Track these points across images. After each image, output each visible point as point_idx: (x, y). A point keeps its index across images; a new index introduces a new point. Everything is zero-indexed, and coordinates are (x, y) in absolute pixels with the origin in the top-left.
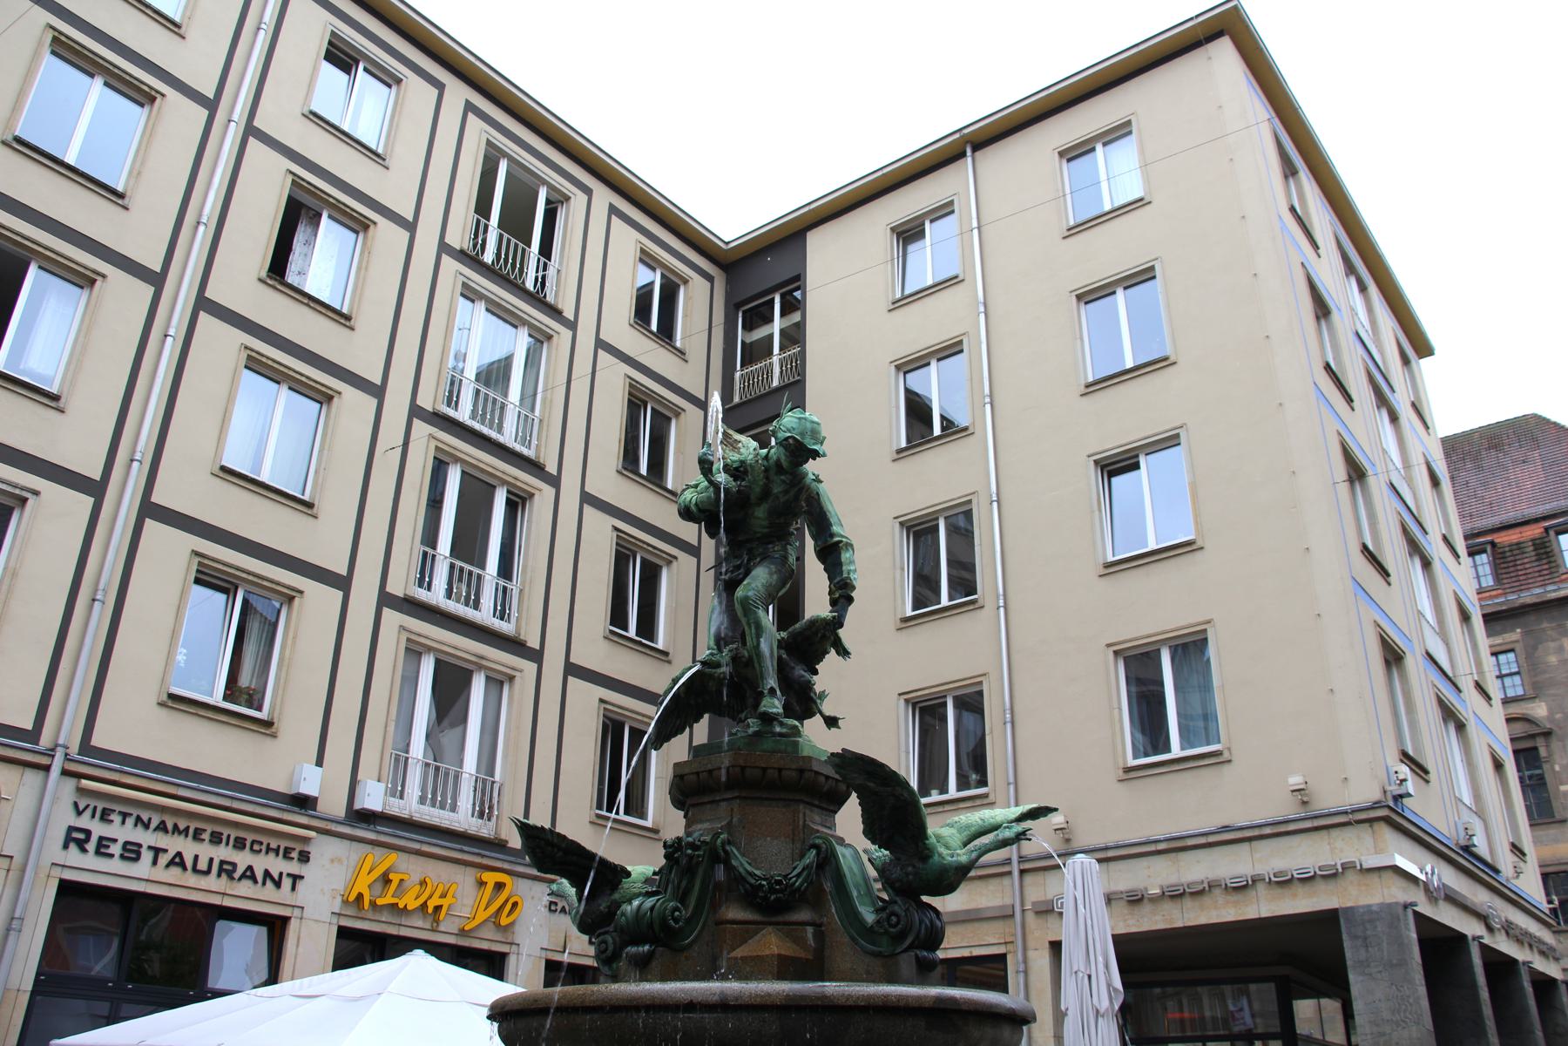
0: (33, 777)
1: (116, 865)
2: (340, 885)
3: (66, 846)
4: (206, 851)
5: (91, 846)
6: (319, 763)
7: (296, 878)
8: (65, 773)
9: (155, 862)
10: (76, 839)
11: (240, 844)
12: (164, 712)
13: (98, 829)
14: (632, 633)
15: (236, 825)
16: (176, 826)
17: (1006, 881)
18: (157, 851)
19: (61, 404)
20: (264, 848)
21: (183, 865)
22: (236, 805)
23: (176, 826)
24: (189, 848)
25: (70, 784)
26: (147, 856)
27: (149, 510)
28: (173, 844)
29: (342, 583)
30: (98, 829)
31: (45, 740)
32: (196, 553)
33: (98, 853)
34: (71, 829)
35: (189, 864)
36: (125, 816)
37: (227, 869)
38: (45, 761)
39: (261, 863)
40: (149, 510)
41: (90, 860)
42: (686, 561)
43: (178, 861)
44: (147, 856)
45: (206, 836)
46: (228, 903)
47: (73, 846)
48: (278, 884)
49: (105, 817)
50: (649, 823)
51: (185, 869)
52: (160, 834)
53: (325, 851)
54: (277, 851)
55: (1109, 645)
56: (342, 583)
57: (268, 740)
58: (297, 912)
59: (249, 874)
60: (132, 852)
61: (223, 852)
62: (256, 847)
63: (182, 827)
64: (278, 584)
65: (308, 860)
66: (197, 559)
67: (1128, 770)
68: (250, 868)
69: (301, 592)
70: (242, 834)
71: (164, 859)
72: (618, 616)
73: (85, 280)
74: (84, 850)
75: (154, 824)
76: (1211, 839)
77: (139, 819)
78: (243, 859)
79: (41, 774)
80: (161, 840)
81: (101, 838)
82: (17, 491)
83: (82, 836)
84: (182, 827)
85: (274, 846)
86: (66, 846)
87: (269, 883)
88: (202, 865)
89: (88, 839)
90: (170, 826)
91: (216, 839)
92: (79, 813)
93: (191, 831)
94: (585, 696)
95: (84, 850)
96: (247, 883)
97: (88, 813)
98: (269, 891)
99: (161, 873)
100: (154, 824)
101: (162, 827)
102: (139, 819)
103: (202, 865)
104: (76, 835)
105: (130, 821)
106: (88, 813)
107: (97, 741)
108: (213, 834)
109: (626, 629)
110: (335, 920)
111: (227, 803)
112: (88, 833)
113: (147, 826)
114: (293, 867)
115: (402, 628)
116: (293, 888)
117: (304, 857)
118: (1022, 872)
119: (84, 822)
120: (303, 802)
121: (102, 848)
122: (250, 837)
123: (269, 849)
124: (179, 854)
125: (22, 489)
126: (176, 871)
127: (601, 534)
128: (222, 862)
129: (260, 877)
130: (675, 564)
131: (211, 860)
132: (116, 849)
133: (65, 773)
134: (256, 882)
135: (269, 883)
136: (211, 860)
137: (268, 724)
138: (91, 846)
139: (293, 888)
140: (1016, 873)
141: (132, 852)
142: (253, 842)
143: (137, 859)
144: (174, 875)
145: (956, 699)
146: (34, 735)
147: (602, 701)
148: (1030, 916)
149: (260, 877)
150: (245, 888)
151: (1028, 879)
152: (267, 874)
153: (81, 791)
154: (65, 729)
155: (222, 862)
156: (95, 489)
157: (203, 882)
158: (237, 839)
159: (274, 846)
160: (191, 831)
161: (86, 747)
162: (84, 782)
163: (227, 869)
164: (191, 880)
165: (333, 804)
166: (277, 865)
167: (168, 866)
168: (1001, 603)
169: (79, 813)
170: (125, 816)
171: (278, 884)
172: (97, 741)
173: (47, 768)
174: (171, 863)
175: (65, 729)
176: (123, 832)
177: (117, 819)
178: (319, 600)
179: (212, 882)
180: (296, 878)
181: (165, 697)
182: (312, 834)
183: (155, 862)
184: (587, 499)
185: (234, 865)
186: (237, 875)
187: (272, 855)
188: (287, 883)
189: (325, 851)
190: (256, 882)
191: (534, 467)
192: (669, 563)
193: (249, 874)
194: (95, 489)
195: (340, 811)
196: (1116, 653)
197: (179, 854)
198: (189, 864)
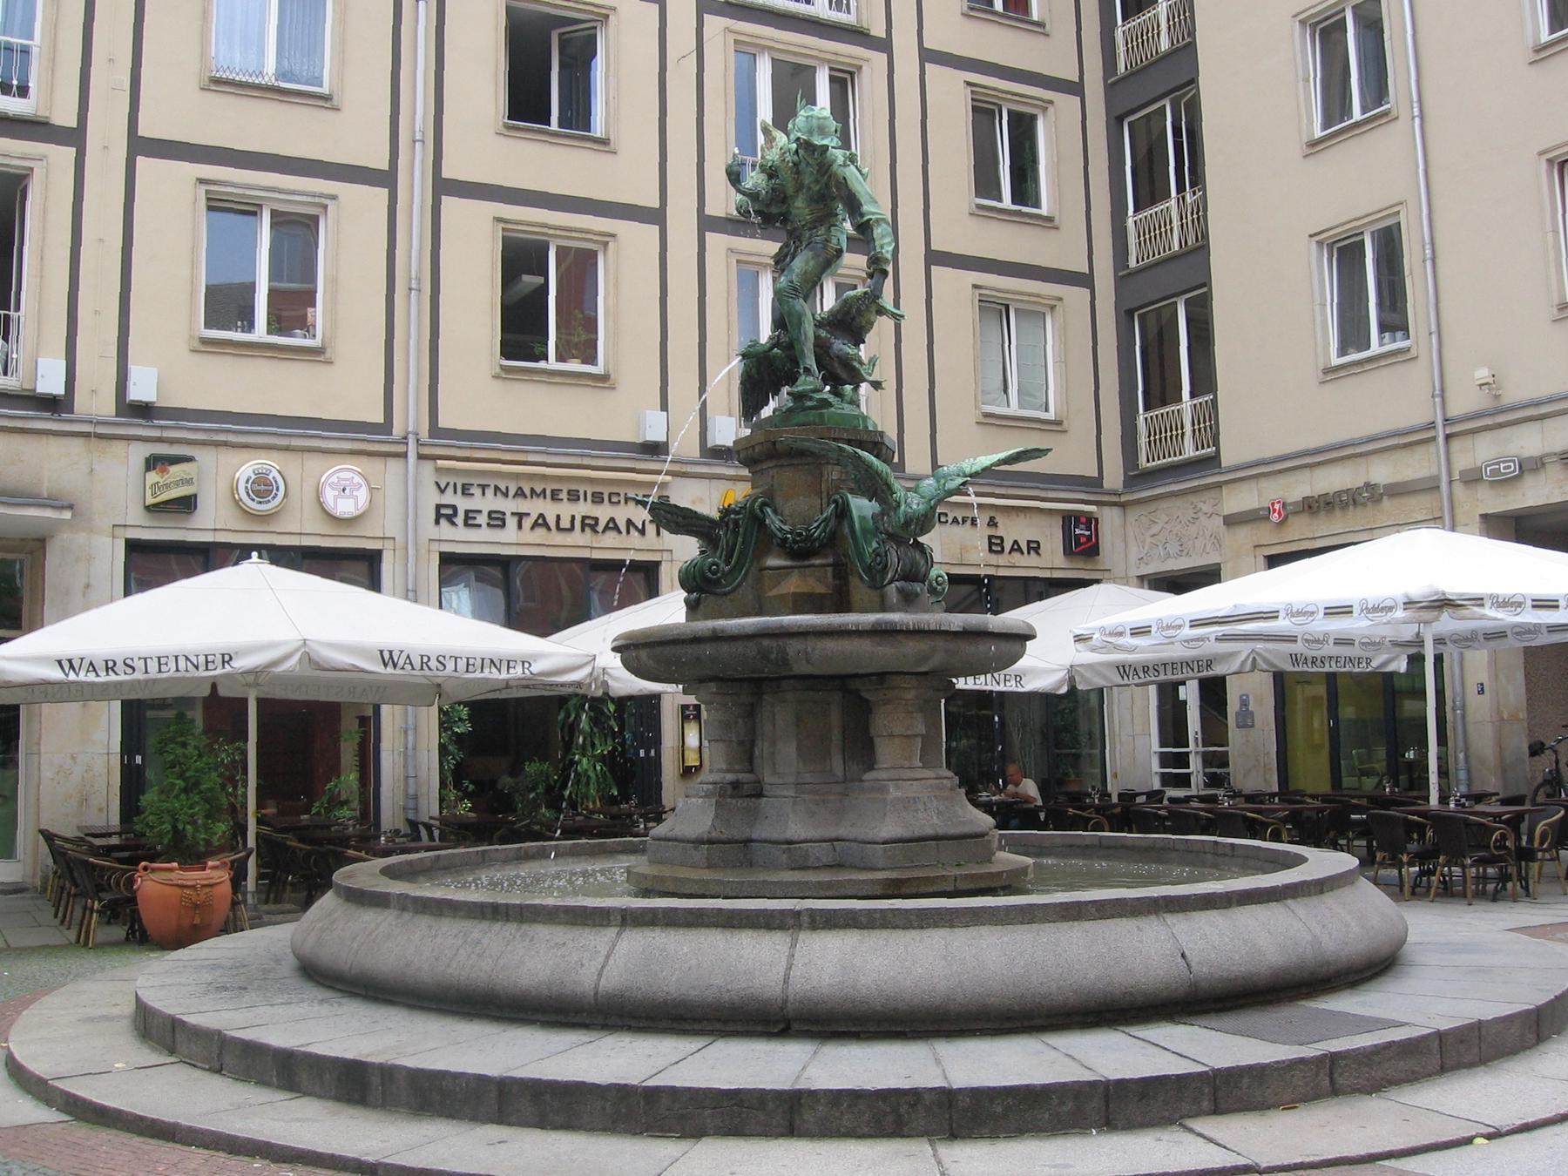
0: (394, 465)
1: (485, 534)
3: (437, 522)
4: (566, 510)
5: (460, 520)
6: (664, 406)
8: (421, 457)
9: (520, 526)
10: (445, 514)
11: (598, 499)
12: (498, 384)
13: (463, 504)
14: (1007, 201)
15: (591, 480)
16: (532, 490)
17: (1432, 448)
18: (521, 517)
19: (335, 102)
21: (546, 525)
22: (586, 461)
23: (532, 490)
24: (550, 510)
25: (428, 466)
26: (512, 522)
27: (444, 187)
28: (534, 507)
29: (656, 216)
31: (397, 430)
32: (498, 220)
33: (466, 524)
34: (438, 507)
36: (483, 487)
37: (590, 524)
38: (401, 449)
40: (444, 187)
41: (461, 533)
42: (1067, 104)
43: (541, 522)
44: (512, 522)
45: (564, 496)
46: (597, 555)
47: (443, 522)
49: (466, 491)
50: (1051, 415)
51: (549, 529)
52: (520, 500)
55: (1541, 154)
56: (656, 216)
57: (607, 393)
58: (666, 556)
59: (612, 526)
60: (497, 520)
61: (584, 508)
62: (614, 499)
63: (538, 490)
64: (588, 232)
67: (1329, 370)
68: (612, 520)
69: (613, 236)
70: (598, 489)
71: (527, 523)
72: (985, 183)
74: (454, 524)
75: (512, 492)
76: (1544, 410)
77: (497, 488)
78: (603, 513)
79: (402, 460)
80: (523, 506)
81: (467, 512)
82: (317, 200)
83: (450, 512)
84: (538, 490)
86: (437, 522)
87: (632, 530)
88: (565, 523)
89: (455, 513)
90: (527, 492)
91: (574, 496)
92: (442, 491)
93: (548, 493)
94: (954, 286)
95: (454, 524)
96: (611, 534)
97: (450, 490)
99: (529, 536)
100: (512, 492)
101: (520, 493)
102: (497, 488)
103: (565, 523)
104: (443, 511)
105: (490, 492)
106: (450, 490)
108: (569, 492)
109: (1000, 199)
111: (578, 461)
112: (454, 508)
113: (506, 495)
115: (731, 250)
118: (1448, 437)
119: (449, 498)
120: (655, 449)
121: (470, 519)
122: (606, 491)
123: (627, 500)
124: (541, 516)
125: (321, 196)
126: (541, 531)
127: (951, 94)
128: (584, 518)
129: (623, 528)
130: (1051, 109)
131: (573, 517)
132: (482, 519)
133: (421, 457)
135: (632, 530)
136: (573, 517)
137: (604, 378)
138: (460, 520)
140: (1441, 439)
143: (503, 525)
144: (540, 535)
146: (386, 427)
147: (975, 287)
148: (1459, 489)
149: (623, 528)
150: (610, 539)
151: (1456, 445)
152: (629, 523)
153: (438, 470)
154: (410, 417)
155: (584, 518)
156: (386, 179)
157: (568, 539)
160: (548, 493)
161: (436, 431)
162: (439, 462)
163: (590, 524)
164: (559, 538)
165: (685, 444)
167: (532, 528)
168: (1416, 111)
169: (442, 491)
170: (483, 487)
173: (405, 455)
174: (535, 525)
175: (410, 417)
176: (486, 503)
177: (477, 491)
178: (637, 239)
179: (577, 538)
181: (498, 370)
183: (520, 526)
184: (928, 56)
185: (596, 519)
186: (600, 528)
191: (856, 35)
192: (1045, 109)
193: (612, 526)
194: (386, 179)
195: (694, 451)
196: (1550, 161)
197: (541, 516)
198: (552, 522)
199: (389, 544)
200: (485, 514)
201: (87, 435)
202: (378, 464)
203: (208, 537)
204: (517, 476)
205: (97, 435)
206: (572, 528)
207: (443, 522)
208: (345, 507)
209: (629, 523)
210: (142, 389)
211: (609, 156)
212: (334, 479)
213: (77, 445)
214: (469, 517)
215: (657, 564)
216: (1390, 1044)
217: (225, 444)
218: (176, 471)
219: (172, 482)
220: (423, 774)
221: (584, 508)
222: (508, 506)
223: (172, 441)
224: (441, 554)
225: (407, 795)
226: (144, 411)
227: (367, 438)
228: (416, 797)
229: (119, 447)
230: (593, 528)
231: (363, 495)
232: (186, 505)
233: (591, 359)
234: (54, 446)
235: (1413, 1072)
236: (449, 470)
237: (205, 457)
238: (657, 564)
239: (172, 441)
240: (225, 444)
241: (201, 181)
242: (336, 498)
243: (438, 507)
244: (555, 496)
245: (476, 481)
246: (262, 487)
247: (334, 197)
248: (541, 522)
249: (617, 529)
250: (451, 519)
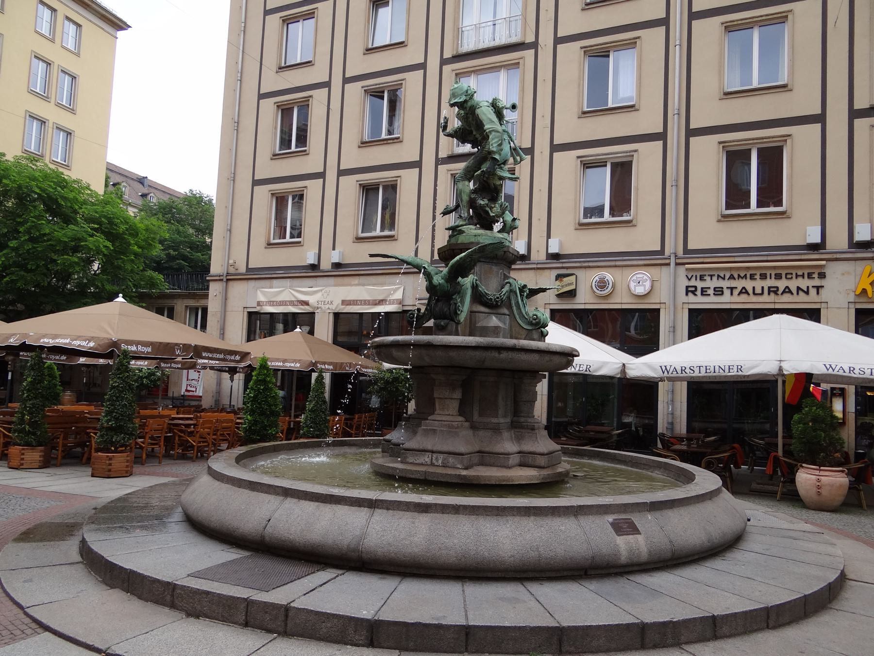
0: (664, 268)
1: (713, 299)
2: (853, 288)
3: (687, 294)
4: (758, 284)
5: (699, 292)
7: (818, 288)
8: (677, 264)
9: (732, 294)
10: (690, 290)
11: (778, 277)
12: (721, 225)
13: (700, 285)
15: (775, 268)
16: (739, 276)
18: (732, 289)
20: (794, 276)
21: (747, 293)
22: (769, 258)
23: (739, 276)
24: (749, 284)
28: (739, 284)
30: (700, 285)
31: (667, 253)
33: (702, 294)
34: (687, 287)
35: (751, 292)
36: (711, 276)
37: (773, 290)
38: (667, 261)
39: (793, 284)
41: (700, 298)
43: (744, 291)
44: (727, 292)
45: (758, 277)
46: (778, 306)
47: (690, 294)
48: (807, 293)
49: (702, 278)
51: (749, 294)
52: (732, 281)
53: (835, 271)
54: (803, 276)
58: (823, 305)
59: (787, 290)
60: (719, 291)
61: (770, 283)
62: (789, 276)
64: (773, 137)
65: (825, 277)
66: (721, 145)
71: (736, 292)
73: (632, 44)
75: (727, 277)
77: (719, 276)
78: (782, 284)
80: (733, 283)
85: (800, 273)
88: (758, 291)
89: (696, 290)
90: (736, 276)
91: (763, 277)
92: (689, 280)
93: (748, 276)
97: (694, 278)
98: (802, 297)
99: (735, 298)
101: (732, 277)
102: (719, 276)
103: (758, 291)
104: (690, 289)
105: (715, 278)
106: (694, 278)
107: (690, 247)
108: (761, 275)
110: (852, 306)
111: (765, 258)
112: (696, 287)
113: (724, 279)
114: (817, 282)
116: (818, 293)
117: (822, 276)
119: (693, 283)
121: (704, 292)
123: (797, 276)
124: (744, 288)
128: (769, 288)
129: (795, 292)
131: (763, 288)
132: (711, 292)
133: (677, 264)
134: (792, 294)
135: (801, 293)
136: (763, 288)
138: (699, 292)
139: (818, 293)
141: (719, 291)
142: (786, 274)
144: (744, 297)
145: (760, 151)
146: (662, 252)
149: (795, 292)
150: (787, 298)
152: (799, 289)
155: (769, 288)
158: (776, 275)
159: (800, 273)
160: (748, 276)
161: (686, 251)
163: (773, 290)
166: (804, 283)
169: (689, 280)
170: (711, 276)
171: (807, 293)
172: (690, 247)
176: (711, 284)
177: (708, 278)
179: (766, 298)
180: (818, 288)
181: (720, 217)
182: (824, 263)
183: (732, 294)
185: (777, 288)
187: (800, 279)
188: (813, 292)
189: (835, 271)
190: (792, 294)
193: (787, 290)
195: (844, 244)
197: (744, 288)
198: (751, 292)
199: (663, 306)
200: (712, 289)
201: (534, 269)
202: (657, 269)
203: (582, 307)
204: (731, 269)
205: (540, 268)
206: (762, 293)
207: (690, 294)
208: (640, 290)
209: (799, 289)
210: (554, 249)
211: (788, 93)
212: (634, 278)
213: (531, 273)
214: (704, 292)
215: (819, 310)
216: (208, 593)
217: (589, 267)
218: (566, 280)
219: (568, 284)
220: (678, 413)
221: (770, 283)
222: (725, 284)
223: (567, 268)
224: (689, 309)
225: (668, 423)
226: (556, 257)
227: (651, 258)
228: (672, 424)
229: (547, 272)
230: (776, 293)
231: (648, 285)
232: (572, 294)
233: (779, 203)
234: (524, 273)
235: (222, 616)
236: (693, 269)
237: (580, 273)
238: (819, 310)
239: (567, 268)
240: (589, 267)
241: (578, 157)
242: (635, 286)
243: (687, 287)
244: (752, 277)
245: (707, 273)
246: (602, 284)
247: (636, 151)
248: (744, 291)
249: (791, 292)
250: (694, 293)
